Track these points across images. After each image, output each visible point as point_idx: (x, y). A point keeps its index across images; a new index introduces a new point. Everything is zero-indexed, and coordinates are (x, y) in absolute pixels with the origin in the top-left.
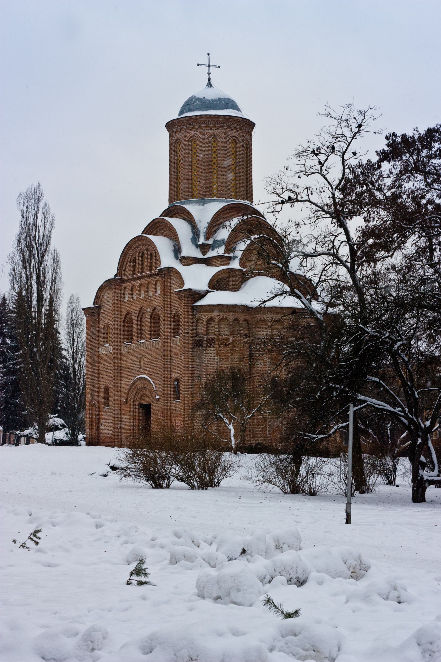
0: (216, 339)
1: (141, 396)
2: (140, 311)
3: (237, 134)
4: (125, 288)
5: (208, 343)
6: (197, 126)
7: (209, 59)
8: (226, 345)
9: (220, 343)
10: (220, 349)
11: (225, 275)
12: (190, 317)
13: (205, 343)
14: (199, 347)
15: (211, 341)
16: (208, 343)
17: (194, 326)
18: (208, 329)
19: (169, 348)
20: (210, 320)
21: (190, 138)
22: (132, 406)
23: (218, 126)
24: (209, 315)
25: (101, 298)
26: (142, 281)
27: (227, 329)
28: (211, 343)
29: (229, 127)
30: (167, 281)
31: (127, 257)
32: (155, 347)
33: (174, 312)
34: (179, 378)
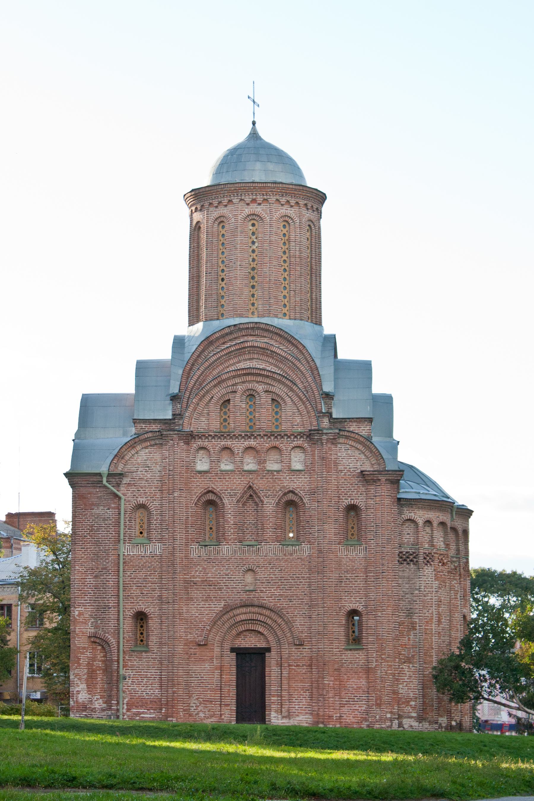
0: (434, 553)
1: (239, 634)
2: (245, 492)
14: (408, 564)
15: (427, 556)
16: (425, 558)
22: (217, 650)
24: (427, 516)
26: (252, 443)
28: (429, 559)
31: (207, 398)
32: (291, 555)
33: (347, 502)
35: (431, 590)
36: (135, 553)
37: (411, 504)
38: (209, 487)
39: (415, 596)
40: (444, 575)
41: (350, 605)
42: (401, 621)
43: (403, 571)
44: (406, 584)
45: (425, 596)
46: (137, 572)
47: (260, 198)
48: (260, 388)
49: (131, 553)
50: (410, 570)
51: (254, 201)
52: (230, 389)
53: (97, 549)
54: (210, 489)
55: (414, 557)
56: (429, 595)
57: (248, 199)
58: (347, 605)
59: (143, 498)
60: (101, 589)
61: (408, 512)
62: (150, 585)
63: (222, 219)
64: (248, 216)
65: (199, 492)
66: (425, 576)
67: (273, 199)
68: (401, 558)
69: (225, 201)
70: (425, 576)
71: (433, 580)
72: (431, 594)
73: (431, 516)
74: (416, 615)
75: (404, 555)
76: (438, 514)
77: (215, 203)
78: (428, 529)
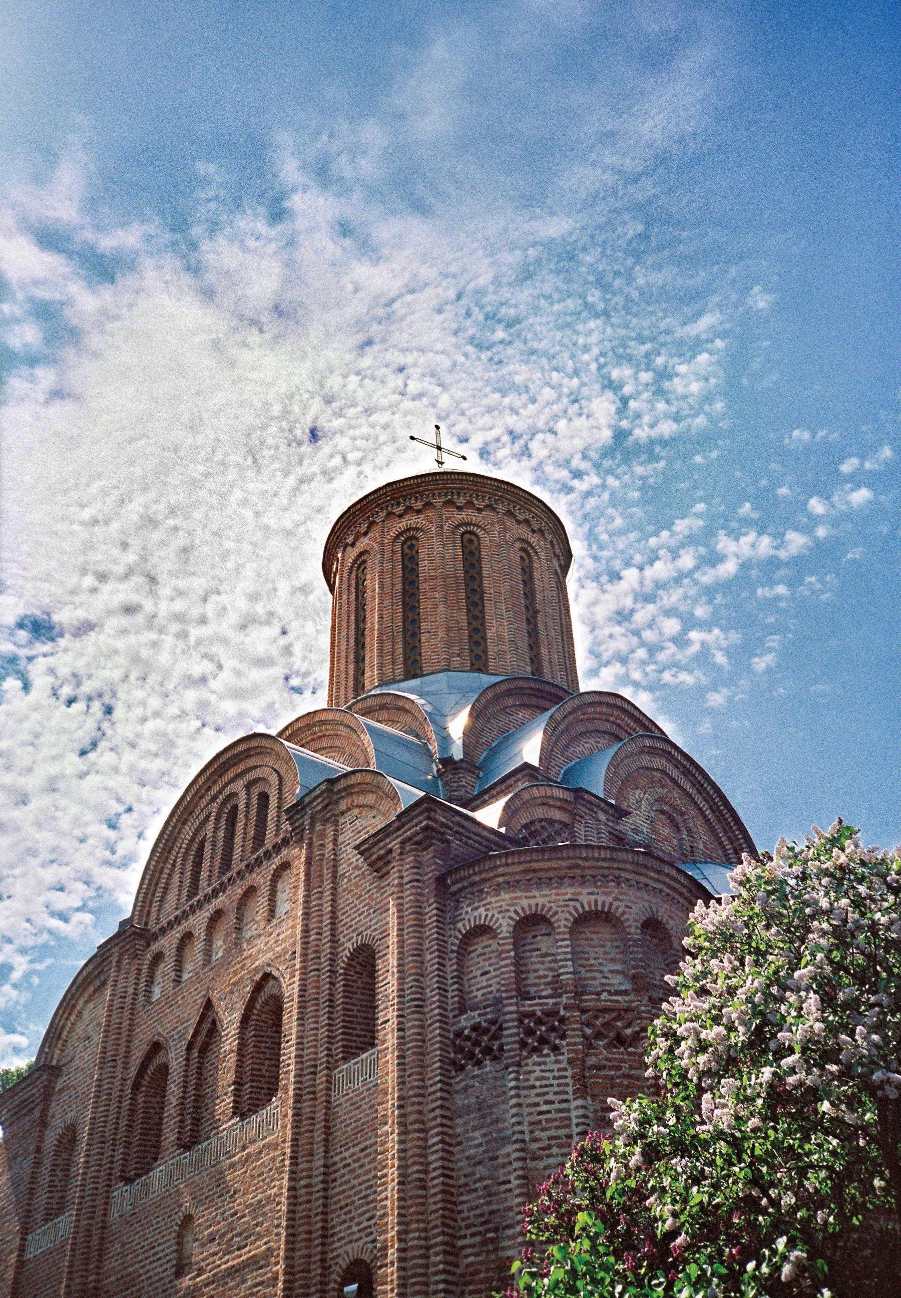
2: (203, 1017)
3: (533, 539)
4: (158, 957)
5: (530, 1032)
6: (419, 505)
7: (438, 434)
8: (620, 1040)
9: (589, 1031)
10: (592, 1061)
11: (557, 815)
12: (431, 932)
13: (511, 1034)
14: (479, 1063)
15: (539, 1022)
17: (451, 968)
18: (519, 964)
19: (320, 1116)
20: (532, 923)
21: (398, 537)
23: (479, 504)
24: (525, 903)
25: (64, 1036)
27: (618, 967)
28: (542, 1032)
29: (509, 513)
30: (323, 835)
34: (367, 1257)
35: (563, 1132)
37: (473, 884)
39: (504, 1166)
40: (624, 1076)
41: (348, 1248)
42: (468, 1266)
43: (465, 1089)
44: (475, 1128)
45: (534, 1159)
50: (483, 1081)
55: (495, 1037)
56: (555, 1150)
58: (339, 1252)
61: (469, 909)
64: (355, 561)
66: (534, 1087)
68: (460, 1050)
70: (534, 1087)
71: (570, 1097)
72: (560, 1146)
73: (541, 901)
74: (510, 1232)
75: (468, 1038)
76: (570, 890)
78: (544, 944)
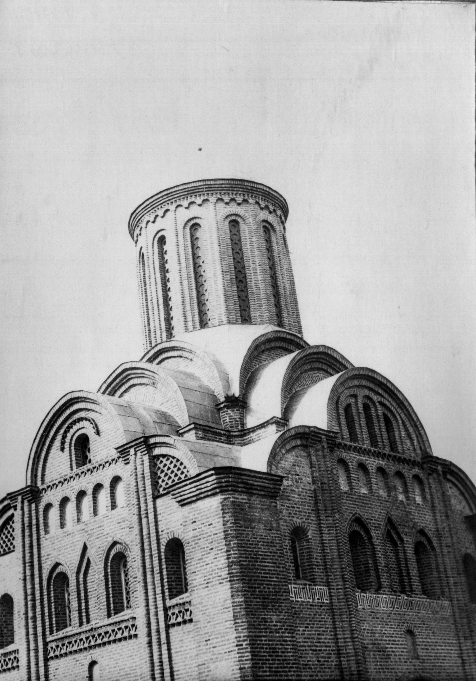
36: (303, 599)
38: (356, 513)
46: (310, 629)
47: (271, 208)
48: (375, 398)
49: (299, 600)
51: (267, 207)
52: (352, 392)
53: (266, 590)
54: (357, 515)
57: (263, 204)
59: (298, 518)
60: (280, 654)
62: (324, 648)
63: (233, 218)
65: (349, 518)
67: (279, 212)
69: (240, 199)
77: (226, 199)
